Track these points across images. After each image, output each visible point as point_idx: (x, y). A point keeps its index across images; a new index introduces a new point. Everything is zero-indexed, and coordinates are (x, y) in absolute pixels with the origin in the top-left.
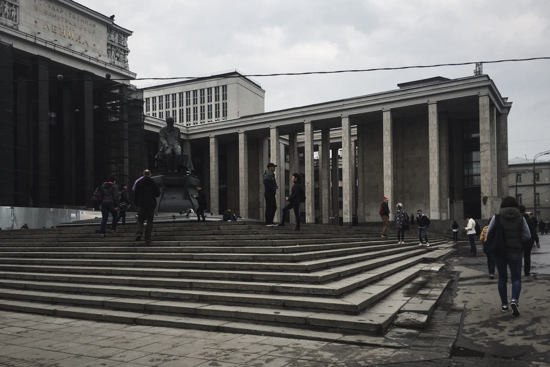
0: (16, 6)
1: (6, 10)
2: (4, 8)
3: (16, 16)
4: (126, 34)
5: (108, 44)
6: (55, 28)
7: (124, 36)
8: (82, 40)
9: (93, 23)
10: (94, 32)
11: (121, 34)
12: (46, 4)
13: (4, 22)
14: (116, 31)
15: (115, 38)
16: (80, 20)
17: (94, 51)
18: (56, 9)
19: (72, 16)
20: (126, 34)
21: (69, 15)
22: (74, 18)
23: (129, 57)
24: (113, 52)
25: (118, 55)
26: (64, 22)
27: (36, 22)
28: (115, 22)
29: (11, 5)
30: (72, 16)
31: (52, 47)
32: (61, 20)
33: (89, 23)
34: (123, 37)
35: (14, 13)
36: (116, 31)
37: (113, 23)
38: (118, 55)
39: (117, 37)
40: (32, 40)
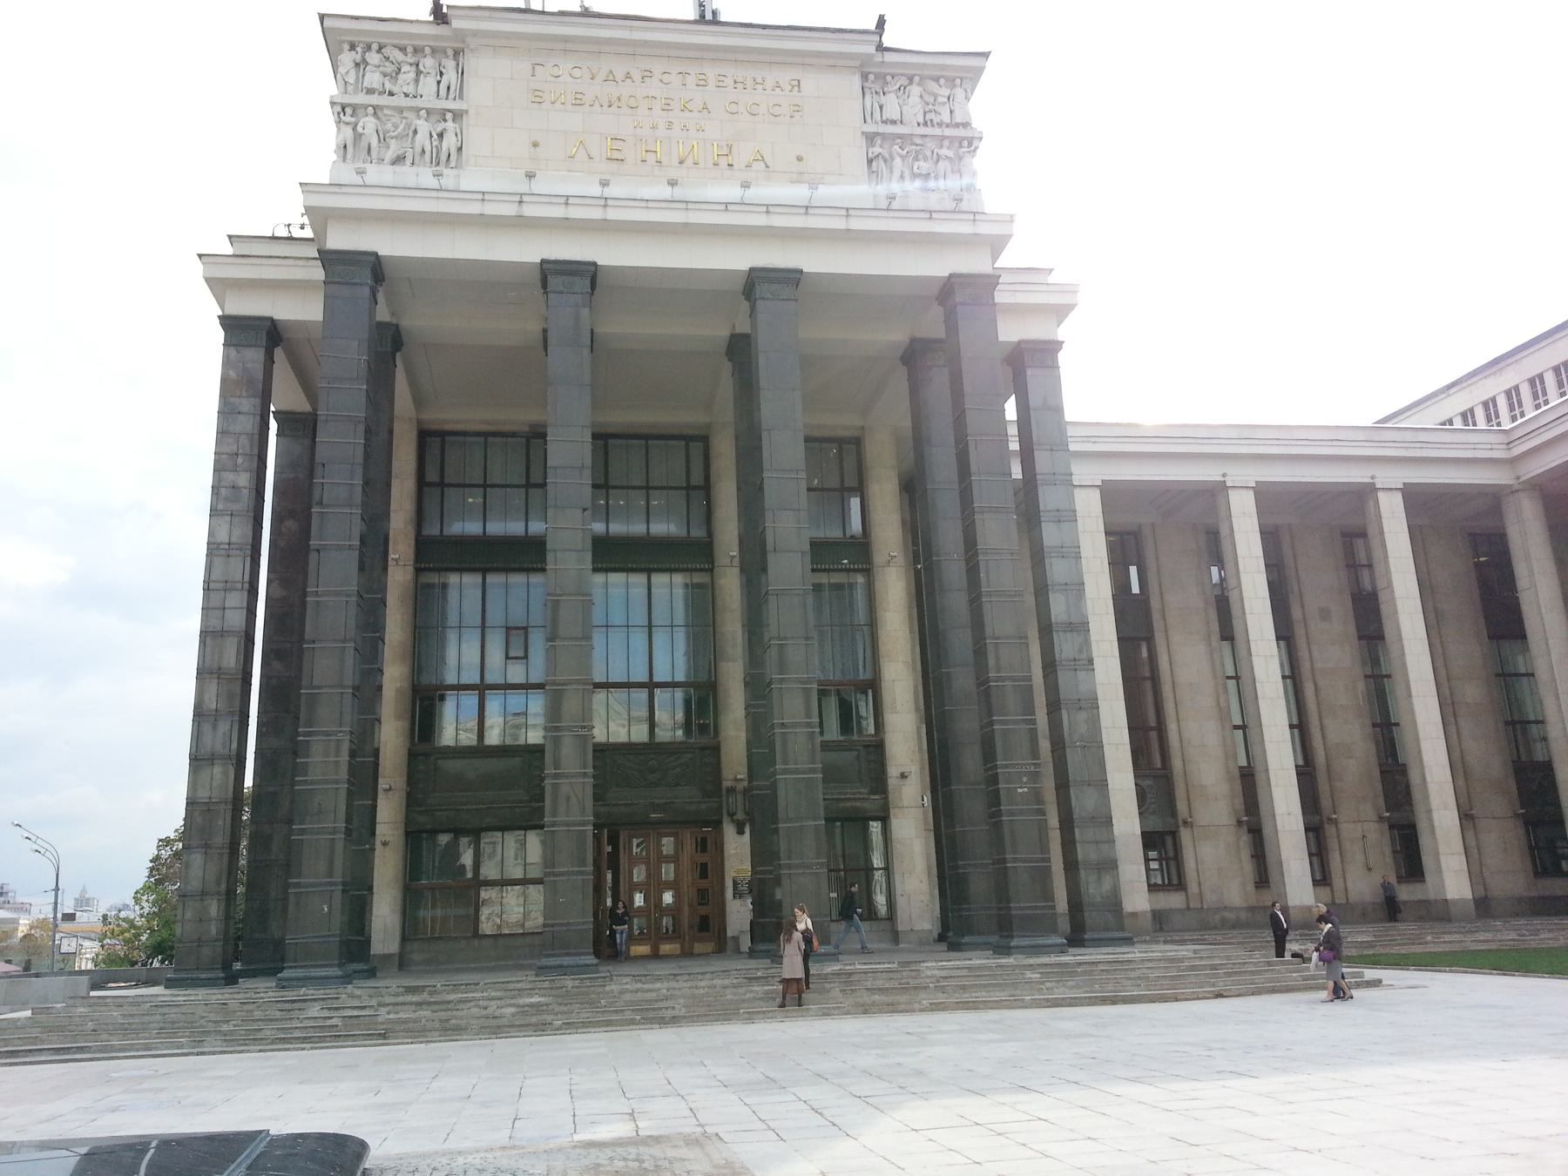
0: (458, 116)
1: (422, 139)
2: (415, 132)
3: (460, 149)
4: (960, 71)
5: (870, 138)
6: (618, 145)
7: (951, 82)
8: (743, 154)
9: (785, 76)
10: (798, 108)
11: (937, 79)
12: (577, 73)
13: (411, 181)
15: (906, 107)
16: (729, 81)
17: (798, 179)
18: (620, 75)
20: (960, 71)
21: (675, 79)
22: (702, 83)
23: (982, 162)
24: (898, 161)
25: (924, 166)
26: (657, 111)
27: (535, 145)
28: (888, 41)
29: (442, 115)
31: (596, 214)
33: (770, 83)
34: (946, 92)
35: (450, 142)
36: (911, 80)
37: (881, 48)
39: (914, 99)
40: (509, 210)
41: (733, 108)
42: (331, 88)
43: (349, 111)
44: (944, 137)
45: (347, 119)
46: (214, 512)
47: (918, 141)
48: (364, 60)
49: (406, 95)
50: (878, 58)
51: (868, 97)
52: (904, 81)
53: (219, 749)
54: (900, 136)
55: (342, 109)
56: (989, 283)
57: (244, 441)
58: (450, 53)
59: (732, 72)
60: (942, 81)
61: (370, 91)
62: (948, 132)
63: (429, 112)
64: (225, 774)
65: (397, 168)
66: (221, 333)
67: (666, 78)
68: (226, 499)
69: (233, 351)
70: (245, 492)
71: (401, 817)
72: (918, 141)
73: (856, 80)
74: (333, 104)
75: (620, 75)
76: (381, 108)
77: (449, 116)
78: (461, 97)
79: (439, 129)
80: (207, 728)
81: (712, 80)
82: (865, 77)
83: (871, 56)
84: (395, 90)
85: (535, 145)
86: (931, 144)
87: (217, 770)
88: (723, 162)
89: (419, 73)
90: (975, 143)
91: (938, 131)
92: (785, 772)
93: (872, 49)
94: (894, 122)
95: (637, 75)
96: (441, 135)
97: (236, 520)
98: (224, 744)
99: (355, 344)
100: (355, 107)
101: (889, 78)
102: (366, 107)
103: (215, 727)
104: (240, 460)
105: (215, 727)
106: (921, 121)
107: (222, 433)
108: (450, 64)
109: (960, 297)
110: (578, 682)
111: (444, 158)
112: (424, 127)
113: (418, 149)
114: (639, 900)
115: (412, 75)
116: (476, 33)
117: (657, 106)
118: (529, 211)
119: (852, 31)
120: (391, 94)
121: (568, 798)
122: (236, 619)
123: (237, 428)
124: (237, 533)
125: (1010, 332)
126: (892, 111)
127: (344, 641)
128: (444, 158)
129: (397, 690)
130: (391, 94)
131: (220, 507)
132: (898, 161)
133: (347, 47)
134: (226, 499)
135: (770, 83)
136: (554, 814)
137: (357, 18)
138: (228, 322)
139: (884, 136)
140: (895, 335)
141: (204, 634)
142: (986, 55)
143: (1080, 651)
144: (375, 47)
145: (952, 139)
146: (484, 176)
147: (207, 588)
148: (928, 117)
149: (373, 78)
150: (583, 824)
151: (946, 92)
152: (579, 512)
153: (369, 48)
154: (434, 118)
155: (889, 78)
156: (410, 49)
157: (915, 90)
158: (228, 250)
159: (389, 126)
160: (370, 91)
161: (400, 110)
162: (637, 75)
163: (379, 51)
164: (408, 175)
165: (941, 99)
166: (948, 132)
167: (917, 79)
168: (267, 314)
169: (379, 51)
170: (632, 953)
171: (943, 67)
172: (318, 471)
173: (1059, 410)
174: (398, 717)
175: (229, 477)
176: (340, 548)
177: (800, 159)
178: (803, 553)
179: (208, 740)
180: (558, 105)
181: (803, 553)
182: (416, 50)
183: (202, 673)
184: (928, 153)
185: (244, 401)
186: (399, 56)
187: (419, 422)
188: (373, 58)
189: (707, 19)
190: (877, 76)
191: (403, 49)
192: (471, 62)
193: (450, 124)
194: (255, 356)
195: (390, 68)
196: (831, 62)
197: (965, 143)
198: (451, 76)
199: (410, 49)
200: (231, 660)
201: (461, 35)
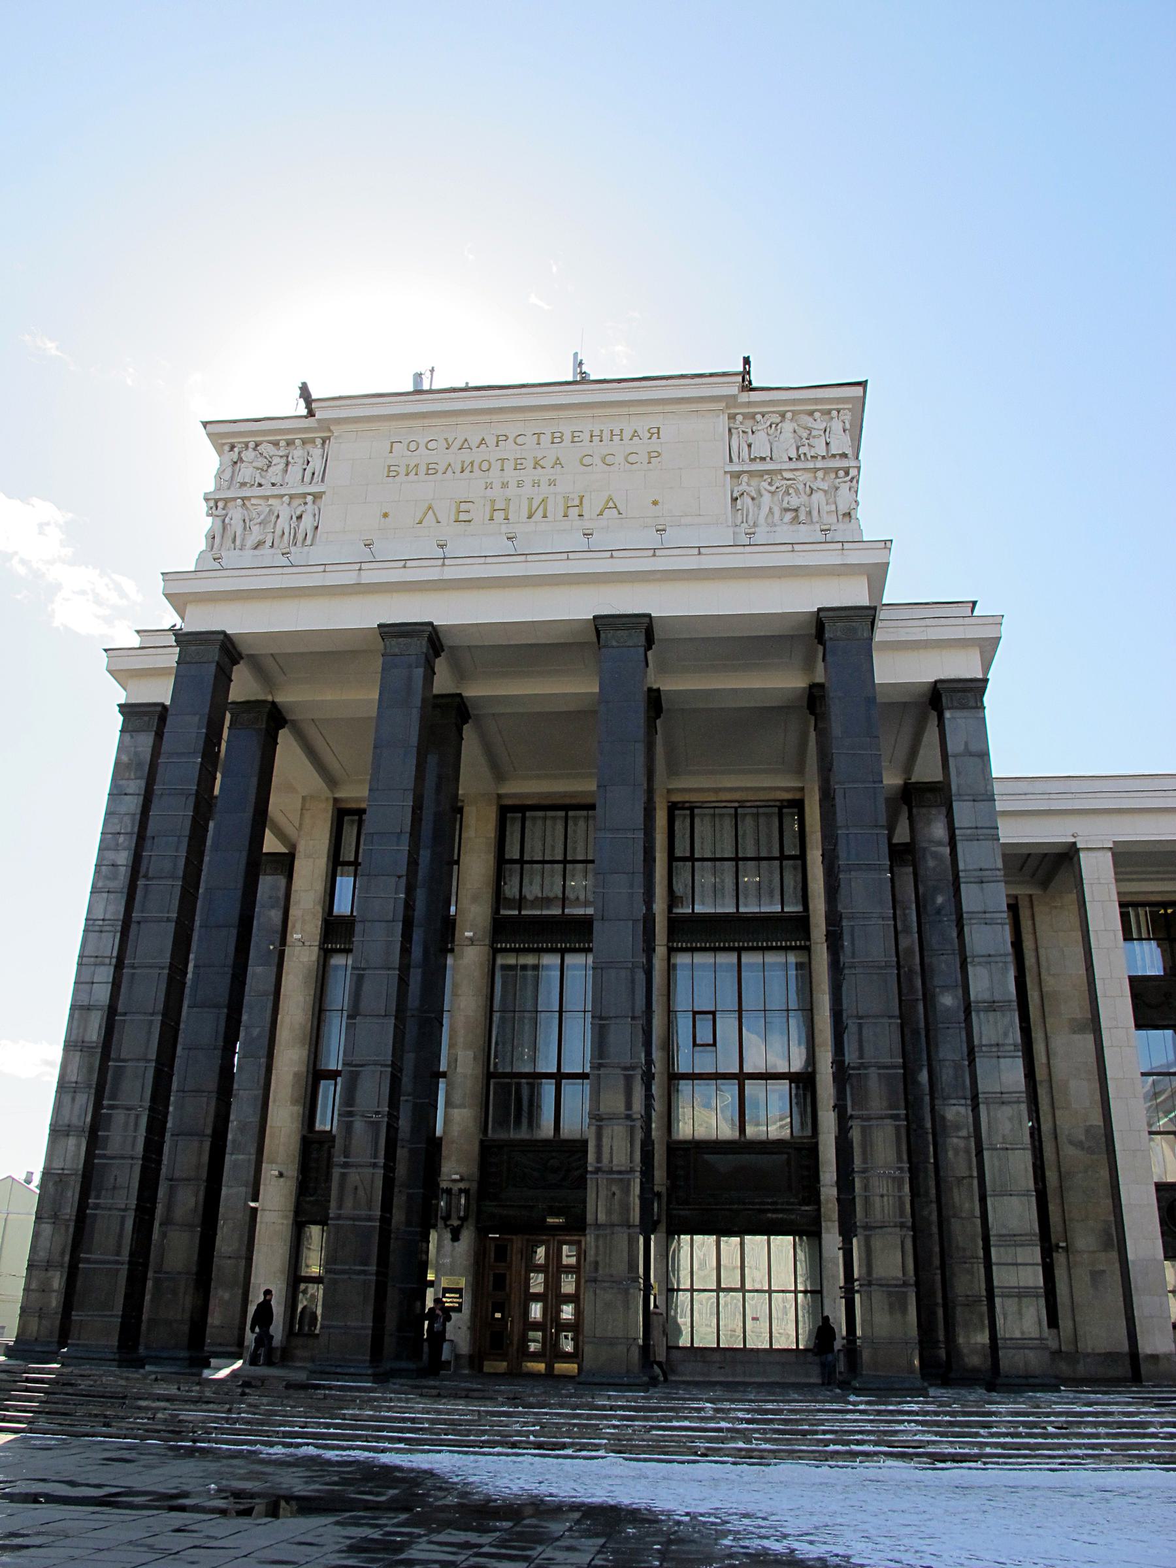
0: (317, 496)
1: (283, 523)
2: (278, 516)
6: (463, 507)
9: (642, 425)
11: (811, 413)
12: (431, 445)
14: (783, 415)
18: (474, 444)
19: (546, 440)
24: (767, 497)
30: (546, 440)
32: (495, 472)
33: (627, 434)
35: (307, 522)
36: (783, 415)
37: (748, 387)
38: (794, 501)
40: (349, 578)
41: (587, 460)
42: (211, 487)
43: (220, 504)
44: (817, 470)
45: (220, 512)
46: (95, 891)
48: (241, 459)
49: (273, 485)
50: (745, 397)
51: (735, 437)
52: (776, 418)
53: (75, 1121)
54: (768, 472)
55: (215, 503)
56: (867, 615)
57: (127, 820)
58: (319, 442)
59: (587, 427)
60: (817, 415)
61: (243, 484)
62: (820, 464)
63: (291, 497)
64: (78, 1146)
65: (256, 552)
66: (121, 718)
67: (520, 440)
68: (107, 878)
69: (127, 736)
70: (123, 869)
71: (290, 1206)
72: (787, 475)
73: (723, 422)
74: (207, 500)
75: (474, 442)
76: (249, 498)
77: (310, 498)
78: (323, 481)
79: (298, 513)
80: (67, 1099)
81: (567, 437)
82: (732, 417)
83: (734, 397)
84: (263, 481)
85: (386, 515)
86: (803, 477)
87: (72, 1141)
88: (574, 512)
89: (287, 464)
90: (853, 472)
91: (811, 465)
92: (598, 1170)
93: (734, 390)
94: (763, 459)
95: (491, 441)
96: (300, 517)
97: (112, 896)
98: (79, 1116)
99: (197, 718)
100: (226, 501)
101: (759, 417)
102: (235, 499)
103: (73, 1099)
104: (121, 839)
105: (73, 1099)
106: (794, 455)
107: (109, 814)
108: (316, 452)
109: (839, 635)
110: (375, 1064)
111: (300, 537)
112: (285, 512)
113: (278, 532)
114: (536, 1311)
115: (282, 466)
116: (339, 421)
117: (509, 466)
118: (368, 577)
120: (260, 485)
121: (356, 1188)
122: (102, 994)
123: (123, 809)
124: (111, 908)
125: (897, 669)
127: (152, 1014)
128: (300, 537)
129: (296, 1074)
130: (260, 485)
131: (100, 884)
132: (767, 497)
133: (227, 448)
134: (107, 878)
135: (627, 434)
136: (340, 1207)
137: (235, 422)
138: (125, 709)
140: (786, 681)
141: (73, 1008)
142: (863, 384)
143: (1006, 1035)
144: (252, 445)
145: (826, 470)
146: (333, 553)
147: (80, 964)
149: (246, 473)
150: (369, 1219)
152: (394, 880)
153: (247, 447)
154: (296, 502)
155: (759, 417)
156: (282, 443)
157: (788, 426)
158: (136, 642)
159: (254, 515)
160: (243, 484)
161: (267, 498)
162: (491, 441)
163: (255, 449)
164: (267, 555)
165: (814, 433)
166: (820, 464)
167: (789, 415)
168: (159, 701)
169: (255, 449)
170: (486, 1369)
171: (816, 401)
172: (148, 843)
173: (983, 756)
174: (295, 1102)
175: (111, 855)
176: (159, 921)
177: (655, 503)
178: (635, 921)
179: (66, 1112)
180: (412, 476)
181: (635, 921)
182: (290, 443)
183: (69, 1046)
184: (801, 487)
185: (131, 783)
186: (271, 450)
187: (336, 800)
188: (248, 455)
189: (584, 380)
190: (745, 416)
191: (276, 444)
192: (332, 446)
193: (310, 507)
194: (146, 741)
195: (261, 463)
196: (694, 407)
197: (841, 473)
198: (316, 464)
199: (282, 443)
200: (94, 1034)
201: (326, 425)
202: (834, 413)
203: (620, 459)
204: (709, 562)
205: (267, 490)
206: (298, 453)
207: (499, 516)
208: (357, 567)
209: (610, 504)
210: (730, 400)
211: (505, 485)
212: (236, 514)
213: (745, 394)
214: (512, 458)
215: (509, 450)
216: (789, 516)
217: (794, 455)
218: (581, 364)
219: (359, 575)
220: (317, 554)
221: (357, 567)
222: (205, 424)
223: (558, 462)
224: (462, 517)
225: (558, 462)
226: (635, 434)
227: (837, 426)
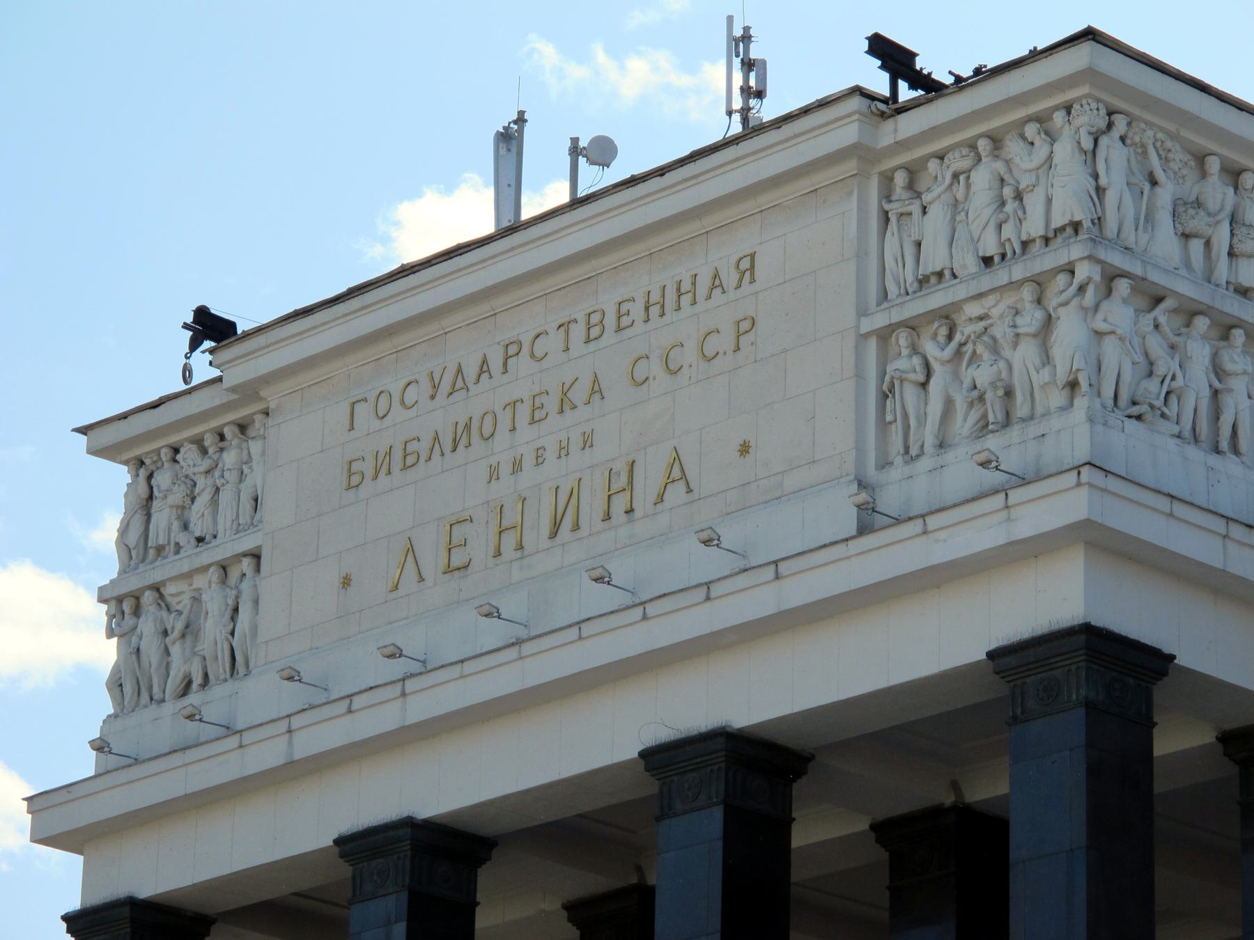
16: (637, 310)
27: (346, 582)
42: (109, 569)
47: (973, 310)
59: (642, 283)
72: (973, 310)
75: (471, 372)
119: (806, 111)
126: (935, 258)
137: (124, 416)
139: (912, 326)
148: (1008, 231)
151: (1041, 152)
157: (982, 178)
162: (496, 363)
167: (983, 145)
196: (805, 185)
202: (1059, 117)
203: (690, 354)
204: (800, 590)
205: (192, 558)
206: (230, 458)
207: (509, 541)
208: (283, 726)
209: (677, 473)
210: (860, 153)
211: (517, 466)
212: (147, 627)
213: (889, 125)
214: (526, 396)
215: (523, 380)
216: (974, 416)
217: (991, 249)
218: (746, 38)
219: (290, 743)
220: (259, 695)
221: (283, 726)
222: (83, 430)
223: (596, 389)
224: (457, 560)
225: (596, 389)
226: (716, 282)
227: (1064, 150)
